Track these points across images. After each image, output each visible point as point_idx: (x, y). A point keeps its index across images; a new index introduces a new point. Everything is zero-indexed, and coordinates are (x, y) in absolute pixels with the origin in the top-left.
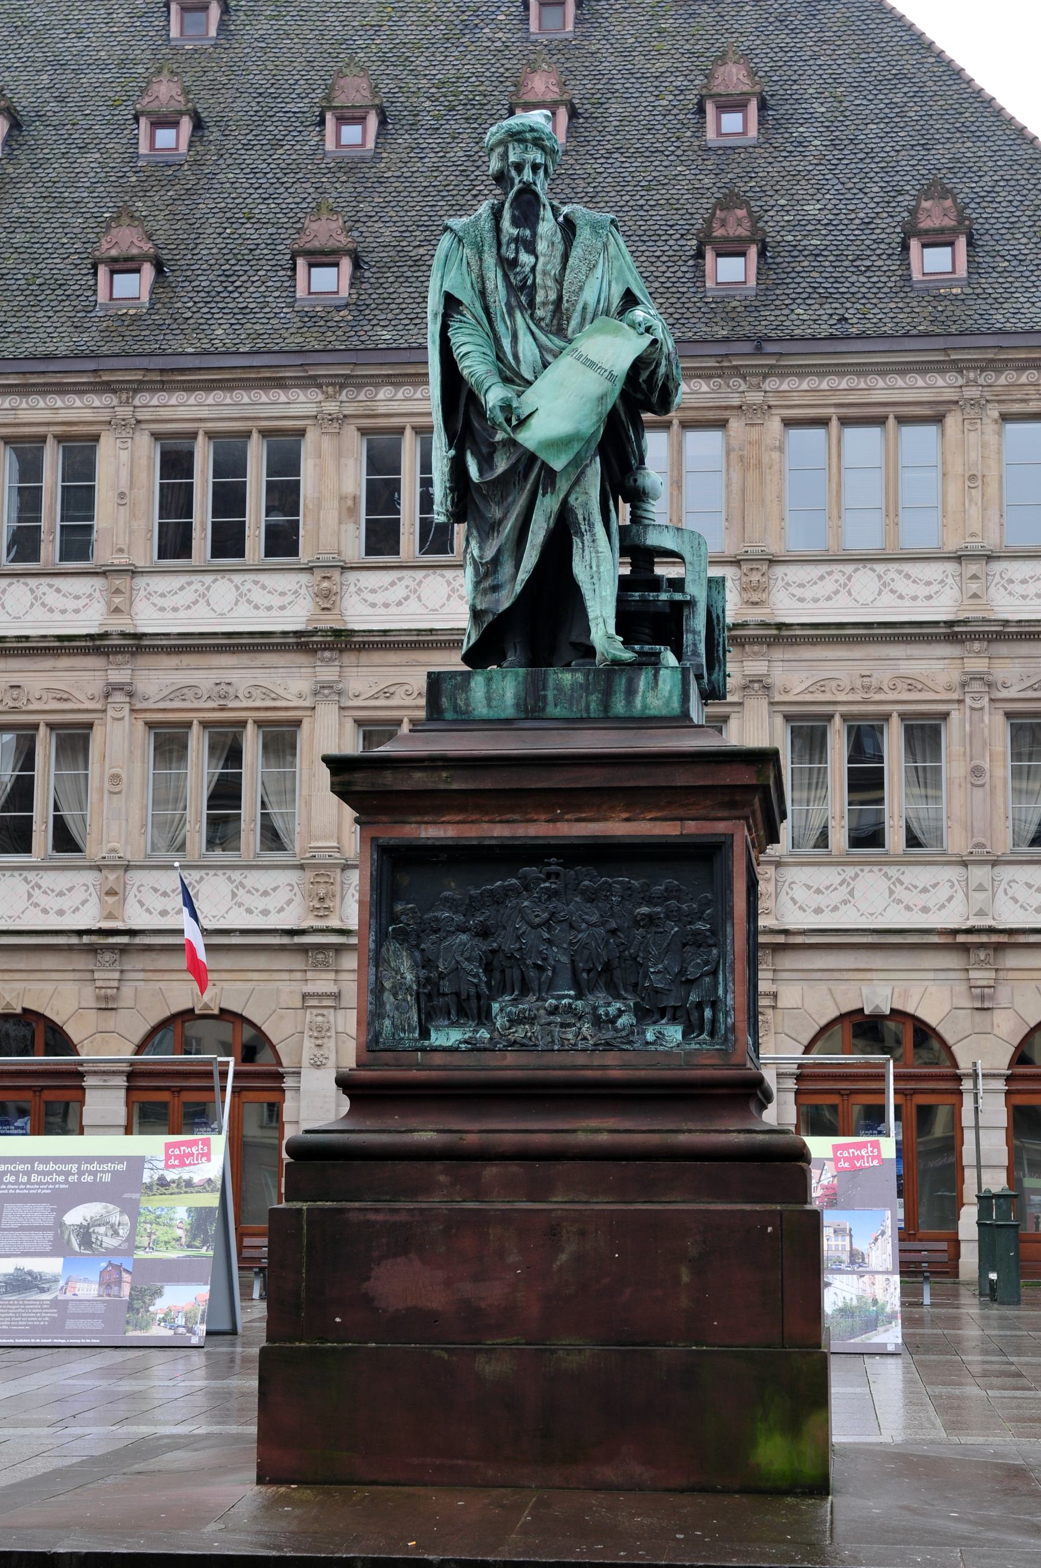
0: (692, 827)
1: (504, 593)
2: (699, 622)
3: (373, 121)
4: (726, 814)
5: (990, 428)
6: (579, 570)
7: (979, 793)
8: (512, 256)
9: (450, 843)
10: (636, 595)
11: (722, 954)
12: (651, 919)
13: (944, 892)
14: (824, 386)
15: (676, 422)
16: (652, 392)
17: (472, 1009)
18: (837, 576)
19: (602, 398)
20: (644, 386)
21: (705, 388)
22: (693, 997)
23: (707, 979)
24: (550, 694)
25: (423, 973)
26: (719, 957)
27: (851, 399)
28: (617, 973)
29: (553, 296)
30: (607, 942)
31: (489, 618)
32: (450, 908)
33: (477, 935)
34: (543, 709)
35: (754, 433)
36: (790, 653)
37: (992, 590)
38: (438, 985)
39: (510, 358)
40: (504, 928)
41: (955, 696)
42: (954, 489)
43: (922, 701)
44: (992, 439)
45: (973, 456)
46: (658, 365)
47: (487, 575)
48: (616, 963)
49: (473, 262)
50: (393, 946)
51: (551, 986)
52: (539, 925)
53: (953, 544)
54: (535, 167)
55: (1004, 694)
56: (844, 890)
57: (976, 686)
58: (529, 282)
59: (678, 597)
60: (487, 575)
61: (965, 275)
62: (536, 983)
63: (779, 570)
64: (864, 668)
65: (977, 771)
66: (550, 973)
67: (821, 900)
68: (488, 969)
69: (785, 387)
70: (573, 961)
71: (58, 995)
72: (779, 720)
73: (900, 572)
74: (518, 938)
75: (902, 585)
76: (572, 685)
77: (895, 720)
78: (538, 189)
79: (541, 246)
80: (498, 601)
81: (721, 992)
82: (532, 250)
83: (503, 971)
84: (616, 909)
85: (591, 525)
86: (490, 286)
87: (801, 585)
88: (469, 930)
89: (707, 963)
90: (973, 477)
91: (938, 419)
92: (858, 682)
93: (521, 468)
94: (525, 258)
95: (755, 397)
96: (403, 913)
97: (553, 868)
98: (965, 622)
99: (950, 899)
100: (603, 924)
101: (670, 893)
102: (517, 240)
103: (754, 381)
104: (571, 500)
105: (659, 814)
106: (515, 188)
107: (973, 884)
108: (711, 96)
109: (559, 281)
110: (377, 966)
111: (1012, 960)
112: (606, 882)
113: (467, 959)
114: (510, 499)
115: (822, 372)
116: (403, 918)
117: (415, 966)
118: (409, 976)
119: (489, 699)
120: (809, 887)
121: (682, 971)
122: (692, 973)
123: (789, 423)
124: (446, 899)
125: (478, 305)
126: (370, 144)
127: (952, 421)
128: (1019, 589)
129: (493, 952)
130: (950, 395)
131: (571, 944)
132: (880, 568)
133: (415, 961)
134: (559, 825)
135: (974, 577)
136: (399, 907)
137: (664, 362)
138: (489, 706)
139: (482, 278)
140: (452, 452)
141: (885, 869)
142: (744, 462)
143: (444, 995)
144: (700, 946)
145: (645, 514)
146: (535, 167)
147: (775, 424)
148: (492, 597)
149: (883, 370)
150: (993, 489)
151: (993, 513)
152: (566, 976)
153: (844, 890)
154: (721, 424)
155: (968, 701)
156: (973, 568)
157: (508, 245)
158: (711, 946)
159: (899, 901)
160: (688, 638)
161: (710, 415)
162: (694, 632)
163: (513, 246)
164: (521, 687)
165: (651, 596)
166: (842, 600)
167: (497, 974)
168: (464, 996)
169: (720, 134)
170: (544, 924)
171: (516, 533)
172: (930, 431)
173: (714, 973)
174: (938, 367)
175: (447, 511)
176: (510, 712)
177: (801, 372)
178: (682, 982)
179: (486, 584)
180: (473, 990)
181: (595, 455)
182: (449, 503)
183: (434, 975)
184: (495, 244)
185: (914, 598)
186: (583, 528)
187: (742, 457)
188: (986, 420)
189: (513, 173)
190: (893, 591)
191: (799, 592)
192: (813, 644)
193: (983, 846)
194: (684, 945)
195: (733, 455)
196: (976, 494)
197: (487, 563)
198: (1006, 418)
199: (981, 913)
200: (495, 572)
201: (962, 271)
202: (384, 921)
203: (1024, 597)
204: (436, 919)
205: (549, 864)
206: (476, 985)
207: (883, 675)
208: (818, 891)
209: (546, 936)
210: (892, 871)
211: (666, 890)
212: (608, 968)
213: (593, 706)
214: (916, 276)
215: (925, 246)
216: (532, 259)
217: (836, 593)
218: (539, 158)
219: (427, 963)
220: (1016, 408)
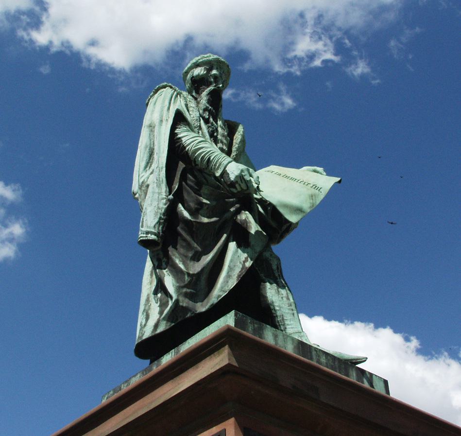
8: (207, 117)
19: (312, 196)
76: (326, 363)
93: (217, 227)
106: (211, 88)
140: (171, 197)
157: (205, 110)
163: (207, 113)
175: (159, 233)
182: (160, 228)
186: (277, 275)
197: (193, 275)
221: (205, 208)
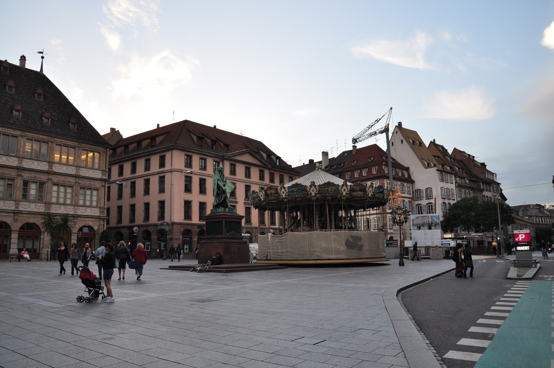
17: (228, 232)
53: (75, 165)
71: (9, 220)
95: (53, 140)
111: (79, 219)
115: (62, 139)
127: (77, 149)
149: (69, 140)
154: (47, 143)
166: (61, 170)
172: (73, 149)
174: (76, 142)
177: (59, 138)
201: (76, 128)
207: (66, 180)
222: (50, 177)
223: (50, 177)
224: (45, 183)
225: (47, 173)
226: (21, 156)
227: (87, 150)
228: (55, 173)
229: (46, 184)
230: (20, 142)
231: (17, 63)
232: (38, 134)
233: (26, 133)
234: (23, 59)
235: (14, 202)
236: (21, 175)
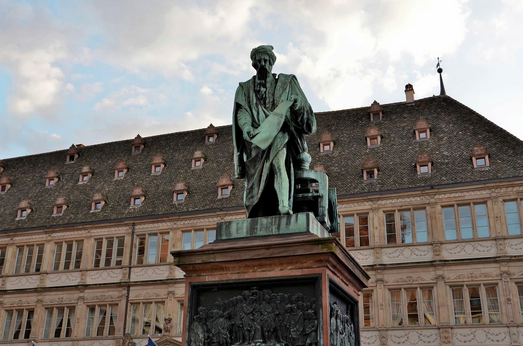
0: (306, 272)
1: (255, 198)
2: (325, 204)
3: (332, 144)
4: (318, 265)
5: (500, 204)
6: (276, 186)
7: (510, 306)
9: (216, 282)
10: (301, 195)
11: (318, 323)
12: (291, 309)
13: (502, 336)
14: (452, 196)
15: (412, 209)
16: (303, 125)
18: (460, 246)
19: (279, 124)
20: (300, 123)
21: (419, 199)
22: (308, 341)
23: (313, 333)
24: (259, 227)
25: (206, 334)
26: (318, 323)
27: (460, 199)
28: (279, 332)
29: (271, 100)
30: (275, 320)
31: (251, 208)
32: (218, 308)
33: (227, 318)
34: (256, 232)
35: (433, 210)
36: (449, 268)
37: (506, 248)
38: (212, 339)
39: (257, 120)
40: (237, 315)
41: (499, 278)
42: (492, 221)
43: (490, 280)
44: (502, 207)
45: (496, 211)
46: (304, 114)
47: (249, 193)
48: (278, 328)
49: (246, 93)
50: (196, 323)
51: (254, 338)
52: (249, 314)
53: (493, 236)
54: (265, 61)
55: (514, 277)
56: (472, 336)
57: (505, 275)
58: (264, 96)
59: (316, 194)
60: (249, 193)
61: (489, 165)
62: (248, 337)
63: (444, 246)
64: (471, 271)
65: (509, 300)
66: (253, 333)
67: (466, 339)
68: (231, 332)
69: (441, 197)
70: (262, 328)
72: (448, 287)
73: (479, 244)
74: (241, 319)
75: (480, 248)
77: (482, 286)
78: (267, 67)
79: (268, 85)
80: (253, 202)
81: (318, 338)
82: (265, 86)
83: (236, 333)
84: (278, 306)
85: (280, 170)
86: (251, 99)
87: (451, 250)
88: (224, 316)
89: (313, 327)
90: (497, 217)
91: (485, 203)
92: (470, 276)
93: (260, 155)
94: (263, 89)
95: (433, 200)
96: (201, 311)
97: (255, 291)
98: (499, 257)
99: (505, 338)
100: (273, 312)
101: (302, 299)
102: (260, 84)
103: (432, 196)
104: (274, 162)
105: (294, 267)
107: (511, 333)
108: (417, 130)
109: (273, 95)
110: (189, 332)
112: (274, 295)
113: (223, 328)
114: (257, 166)
115: (451, 192)
116: (201, 313)
117: (204, 331)
118: (201, 336)
119: (237, 230)
120: (462, 335)
121: (304, 330)
122: (308, 331)
123: (443, 207)
124: (216, 305)
125: (247, 105)
126: (332, 150)
127: (489, 203)
128: (515, 247)
129: (233, 325)
130: (488, 196)
131: (261, 321)
132: (473, 243)
133: (204, 330)
134: (256, 273)
135: (501, 244)
136: (200, 308)
137: (305, 113)
138: (238, 233)
139: (249, 97)
140: (239, 153)
141: (484, 329)
142: (431, 218)
143: (214, 343)
144: (310, 319)
145: (304, 168)
146: (265, 61)
147: (439, 207)
148: (252, 200)
149: (468, 191)
150: (503, 220)
151: (504, 227)
152: (259, 334)
153: (472, 335)
154: (424, 208)
155: (503, 279)
156: (501, 242)
158: (314, 319)
159: (490, 339)
160: (320, 209)
161: (421, 206)
162: (323, 207)
164: (249, 225)
165: (306, 195)
166: (463, 253)
167: (234, 334)
168: (221, 343)
169: (420, 138)
170: (251, 313)
171: (259, 177)
172: (484, 206)
173: (316, 331)
176: (244, 235)
177: (445, 193)
178: (304, 335)
179: (249, 196)
180: (224, 341)
181: (284, 147)
183: (211, 335)
184: (253, 86)
185: (484, 251)
187: (430, 217)
188: (499, 202)
189: (258, 63)
190: (477, 250)
191: (450, 251)
192: (456, 265)
193: (513, 321)
194: (305, 320)
195: (428, 216)
196: (499, 222)
198: (505, 201)
199: (515, 342)
200: (252, 191)
201: (488, 164)
202: (193, 314)
203: (516, 249)
204: (212, 313)
205: (253, 289)
206: (226, 339)
207: (477, 273)
208: (465, 336)
209: (252, 318)
210: (486, 329)
211: (297, 298)
212: (275, 330)
213: (274, 230)
214: (475, 166)
215: (476, 159)
216: (265, 89)
217: (461, 251)
218: (267, 58)
219: (209, 331)
220: (507, 198)
221: (253, 149)
222: (440, 272)
223: (440, 272)
224: (433, 287)
225: (431, 264)
226: (377, 245)
227: (515, 200)
228: (445, 263)
229: (435, 288)
230: (373, 220)
231: (401, 98)
232: (400, 197)
233: (380, 202)
234: (409, 88)
235: (377, 333)
236: (382, 280)
